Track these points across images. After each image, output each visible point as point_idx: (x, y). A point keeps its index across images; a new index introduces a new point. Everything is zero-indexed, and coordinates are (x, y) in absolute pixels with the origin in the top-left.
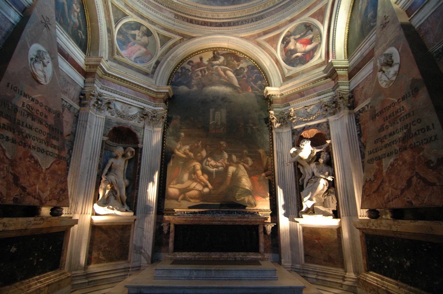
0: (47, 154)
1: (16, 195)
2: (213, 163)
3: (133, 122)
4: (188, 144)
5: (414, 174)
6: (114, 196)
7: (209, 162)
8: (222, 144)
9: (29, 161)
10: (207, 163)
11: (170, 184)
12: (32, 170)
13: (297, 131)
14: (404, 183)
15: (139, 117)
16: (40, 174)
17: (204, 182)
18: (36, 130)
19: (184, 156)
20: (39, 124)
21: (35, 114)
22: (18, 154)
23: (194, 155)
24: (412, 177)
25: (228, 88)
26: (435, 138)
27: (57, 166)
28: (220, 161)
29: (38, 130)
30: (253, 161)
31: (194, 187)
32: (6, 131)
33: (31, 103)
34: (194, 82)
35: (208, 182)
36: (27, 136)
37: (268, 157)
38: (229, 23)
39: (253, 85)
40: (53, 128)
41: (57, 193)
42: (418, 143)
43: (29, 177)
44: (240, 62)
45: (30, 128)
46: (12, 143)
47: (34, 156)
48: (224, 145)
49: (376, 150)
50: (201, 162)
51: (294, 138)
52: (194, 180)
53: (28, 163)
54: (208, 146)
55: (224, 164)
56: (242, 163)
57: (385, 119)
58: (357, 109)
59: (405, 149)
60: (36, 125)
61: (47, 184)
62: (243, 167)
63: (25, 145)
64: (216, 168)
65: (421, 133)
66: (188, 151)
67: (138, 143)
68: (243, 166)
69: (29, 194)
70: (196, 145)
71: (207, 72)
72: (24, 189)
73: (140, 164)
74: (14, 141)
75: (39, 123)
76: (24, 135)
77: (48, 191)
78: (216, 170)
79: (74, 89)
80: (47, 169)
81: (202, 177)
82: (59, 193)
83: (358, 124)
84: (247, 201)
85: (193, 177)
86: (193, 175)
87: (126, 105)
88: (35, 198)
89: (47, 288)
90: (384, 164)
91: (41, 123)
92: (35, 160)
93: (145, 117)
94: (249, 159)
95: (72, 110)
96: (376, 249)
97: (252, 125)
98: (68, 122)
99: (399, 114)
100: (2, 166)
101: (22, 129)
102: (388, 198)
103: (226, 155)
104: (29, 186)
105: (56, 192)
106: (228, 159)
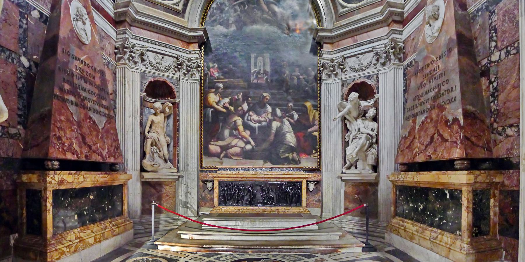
0: (100, 115)
2: (255, 117)
3: (167, 74)
4: (227, 97)
5: (436, 131)
6: (158, 154)
7: (251, 116)
8: (265, 96)
10: (249, 117)
11: (211, 141)
12: (92, 130)
13: (347, 82)
14: (429, 140)
15: (173, 67)
17: (246, 138)
19: (224, 110)
23: (235, 109)
24: (435, 134)
26: (455, 100)
28: (264, 115)
31: (236, 144)
36: (84, 99)
37: (315, 111)
40: (101, 89)
42: (443, 103)
48: (268, 97)
49: (414, 107)
50: (242, 116)
51: (343, 91)
52: (236, 137)
55: (267, 118)
56: (287, 118)
57: (425, 77)
58: (406, 62)
59: (434, 108)
60: (88, 87)
65: (446, 94)
66: (227, 105)
67: (175, 97)
68: (288, 120)
70: (236, 97)
72: (90, 147)
73: (179, 121)
78: (259, 127)
79: (109, 43)
80: (102, 129)
81: (244, 134)
83: (405, 79)
85: (235, 133)
86: (234, 131)
87: (159, 55)
89: (117, 229)
90: (417, 122)
91: (92, 85)
93: (179, 67)
94: (294, 113)
95: (110, 67)
96: (402, 198)
97: (299, 74)
99: (435, 73)
102: (416, 153)
103: (269, 109)
105: (112, 149)
106: (271, 113)
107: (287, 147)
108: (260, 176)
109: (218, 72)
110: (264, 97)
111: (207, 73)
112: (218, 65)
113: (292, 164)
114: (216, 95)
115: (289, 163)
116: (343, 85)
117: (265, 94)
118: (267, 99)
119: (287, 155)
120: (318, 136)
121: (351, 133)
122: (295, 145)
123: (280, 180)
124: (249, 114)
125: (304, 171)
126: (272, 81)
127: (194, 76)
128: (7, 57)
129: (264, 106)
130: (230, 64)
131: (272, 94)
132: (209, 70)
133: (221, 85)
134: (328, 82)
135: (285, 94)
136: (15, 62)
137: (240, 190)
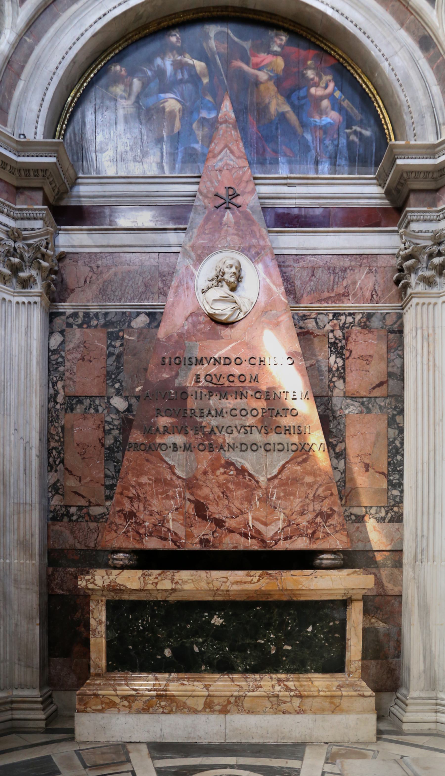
1: (203, 535)
9: (225, 473)
16: (255, 492)
18: (232, 412)
20: (239, 400)
21: (227, 384)
22: (199, 466)
27: (299, 468)
29: (238, 412)
32: (172, 436)
33: (213, 370)
41: (308, 522)
43: (227, 501)
45: (220, 413)
46: (185, 453)
47: (234, 461)
53: (222, 478)
61: (276, 508)
63: (211, 448)
69: (231, 531)
74: (187, 448)
75: (238, 397)
76: (208, 430)
77: (281, 521)
82: (311, 522)
88: (246, 536)
92: (236, 469)
98: (371, 356)
100: (171, 491)
101: (202, 422)
104: (229, 516)
128: (86, 409)
136: (100, 409)
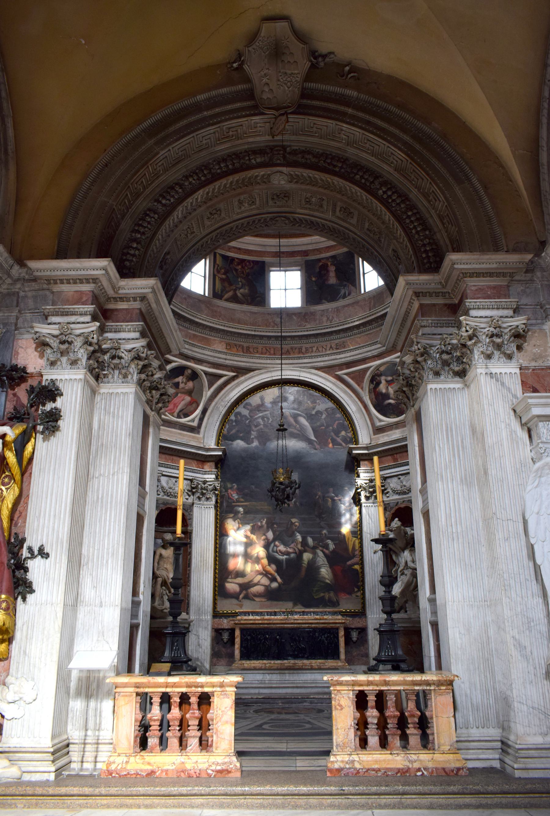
2: (282, 548)
4: (248, 524)
7: (277, 547)
10: (275, 548)
17: (271, 574)
25: (301, 442)
28: (292, 545)
30: (334, 544)
31: (259, 582)
34: (254, 434)
35: (276, 574)
38: (299, 349)
39: (334, 437)
44: (316, 403)
48: (297, 524)
51: (386, 515)
54: (275, 526)
55: (296, 549)
56: (321, 548)
62: (321, 553)
64: (286, 555)
68: (322, 551)
70: (259, 524)
71: (271, 420)
73: (190, 553)
78: (286, 559)
84: (327, 598)
94: (329, 542)
97: (333, 495)
103: (299, 538)
106: (302, 542)
107: (322, 584)
108: (289, 622)
109: (237, 493)
110: (292, 524)
111: (224, 495)
112: (238, 485)
113: (329, 606)
114: (234, 520)
115: (325, 606)
116: (385, 509)
117: (294, 520)
118: (296, 526)
119: (322, 594)
120: (360, 571)
121: (399, 568)
122: (331, 582)
123: (313, 625)
124: (274, 544)
125: (342, 615)
126: (301, 504)
127: (210, 500)
129: (292, 535)
130: (252, 484)
131: (301, 520)
132: (226, 491)
133: (241, 509)
134: (368, 505)
135: (318, 519)
137: (266, 639)
